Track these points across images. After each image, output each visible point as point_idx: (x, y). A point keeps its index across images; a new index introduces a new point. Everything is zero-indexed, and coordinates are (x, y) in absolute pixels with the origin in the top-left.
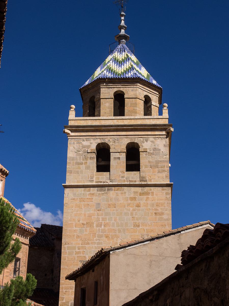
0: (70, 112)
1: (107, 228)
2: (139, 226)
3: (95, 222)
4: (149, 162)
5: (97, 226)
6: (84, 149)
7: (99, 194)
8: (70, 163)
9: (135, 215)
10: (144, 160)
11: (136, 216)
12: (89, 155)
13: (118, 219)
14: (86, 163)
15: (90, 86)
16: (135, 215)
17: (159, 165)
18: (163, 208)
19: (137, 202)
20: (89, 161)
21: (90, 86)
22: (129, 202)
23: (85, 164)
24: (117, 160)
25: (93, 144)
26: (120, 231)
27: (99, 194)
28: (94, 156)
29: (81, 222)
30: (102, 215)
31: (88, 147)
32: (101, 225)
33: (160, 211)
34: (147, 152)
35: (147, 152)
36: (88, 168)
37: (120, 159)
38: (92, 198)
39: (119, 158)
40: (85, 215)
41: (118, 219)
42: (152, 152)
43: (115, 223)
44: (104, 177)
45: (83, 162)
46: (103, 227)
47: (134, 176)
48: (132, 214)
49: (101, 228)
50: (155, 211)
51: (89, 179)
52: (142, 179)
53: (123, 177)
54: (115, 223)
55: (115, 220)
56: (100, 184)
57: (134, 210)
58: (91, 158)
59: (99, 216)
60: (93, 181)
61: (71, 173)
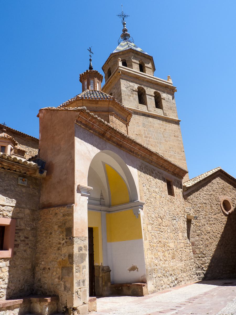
0: (119, 62)
1: (151, 140)
2: (167, 142)
3: (143, 135)
4: (167, 105)
5: (145, 137)
6: (131, 87)
7: (143, 117)
8: (123, 93)
9: (165, 135)
10: (164, 103)
11: (165, 136)
12: (134, 92)
13: (156, 135)
14: (133, 96)
15: (121, 53)
16: (165, 135)
17: (172, 108)
18: (178, 133)
19: (165, 127)
20: (134, 95)
21: (121, 53)
22: (161, 126)
23: (132, 97)
24: (151, 100)
25: (136, 86)
26: (158, 143)
27: (143, 117)
28: (137, 93)
29: (135, 133)
30: (147, 131)
31: (133, 87)
32: (147, 137)
33: (176, 135)
34: (165, 99)
35: (165, 99)
36: (135, 99)
37: (152, 99)
38: (140, 119)
39: (151, 99)
40: (137, 129)
41: (156, 135)
42: (167, 100)
43: (155, 137)
44: (142, 108)
45: (132, 95)
46: (148, 139)
47: (159, 112)
48: (163, 134)
49: (147, 139)
50: (174, 135)
51: (136, 107)
52: (165, 114)
53: (155, 111)
54: (155, 137)
55: (155, 136)
56: (142, 111)
57: (164, 132)
58: (135, 94)
59: (145, 131)
60: (139, 108)
61: (125, 100)
